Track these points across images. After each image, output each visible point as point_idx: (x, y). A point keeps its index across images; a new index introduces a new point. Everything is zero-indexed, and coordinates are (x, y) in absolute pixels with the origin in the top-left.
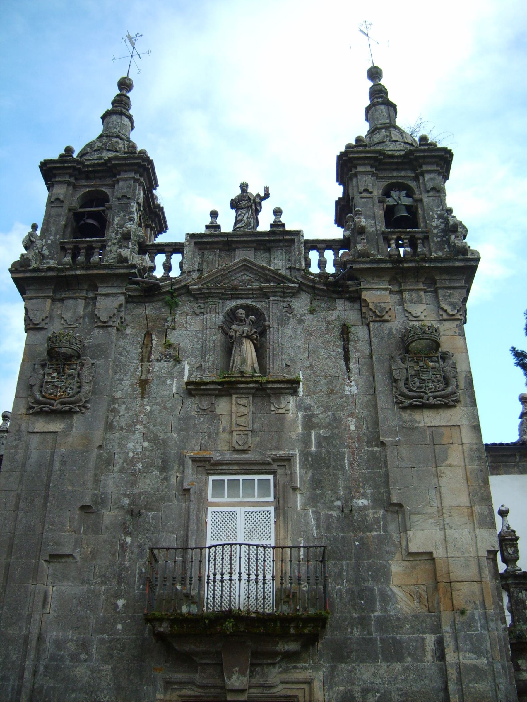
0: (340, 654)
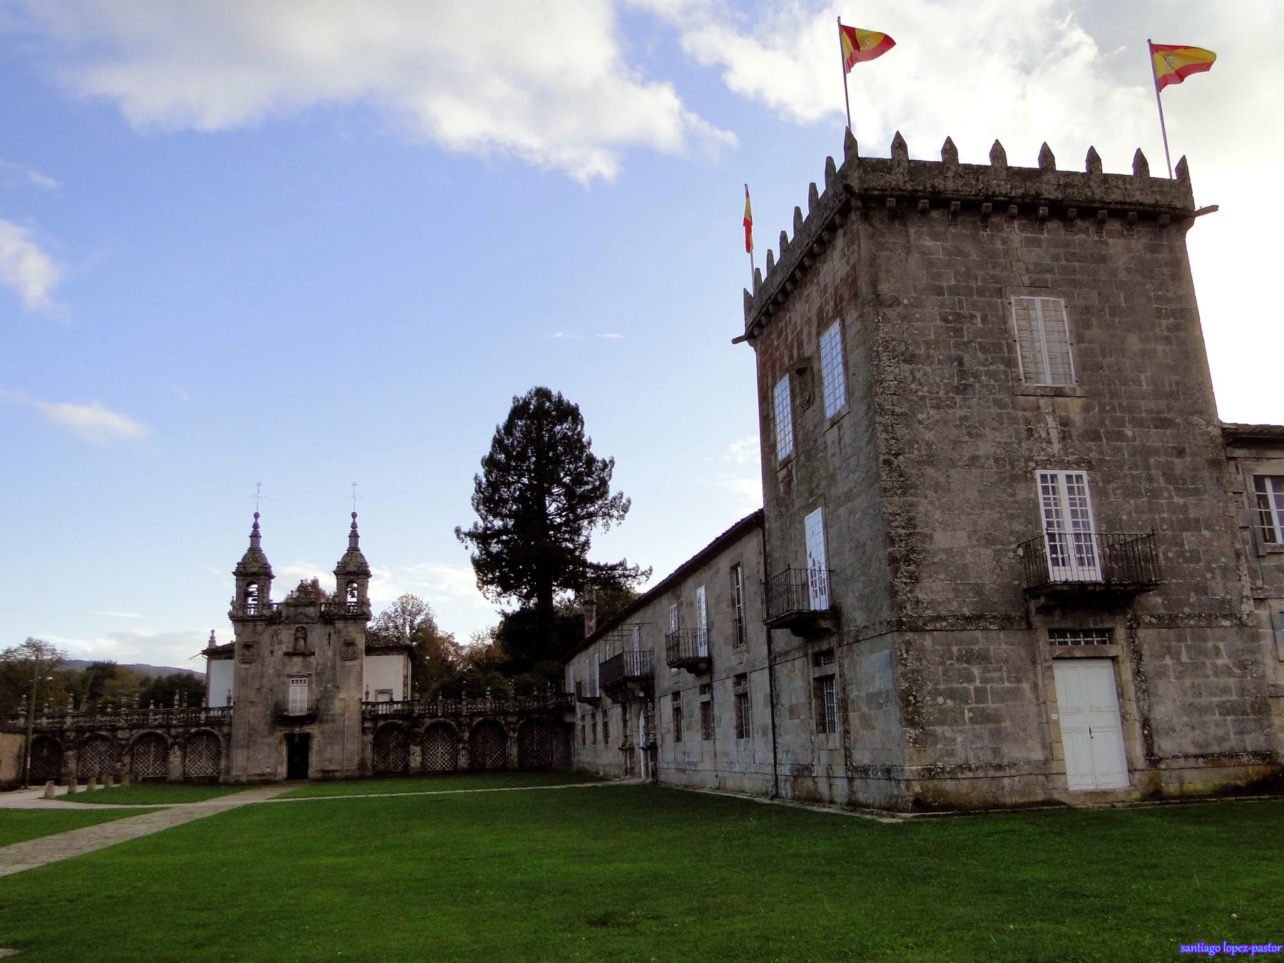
0: (321, 722)
